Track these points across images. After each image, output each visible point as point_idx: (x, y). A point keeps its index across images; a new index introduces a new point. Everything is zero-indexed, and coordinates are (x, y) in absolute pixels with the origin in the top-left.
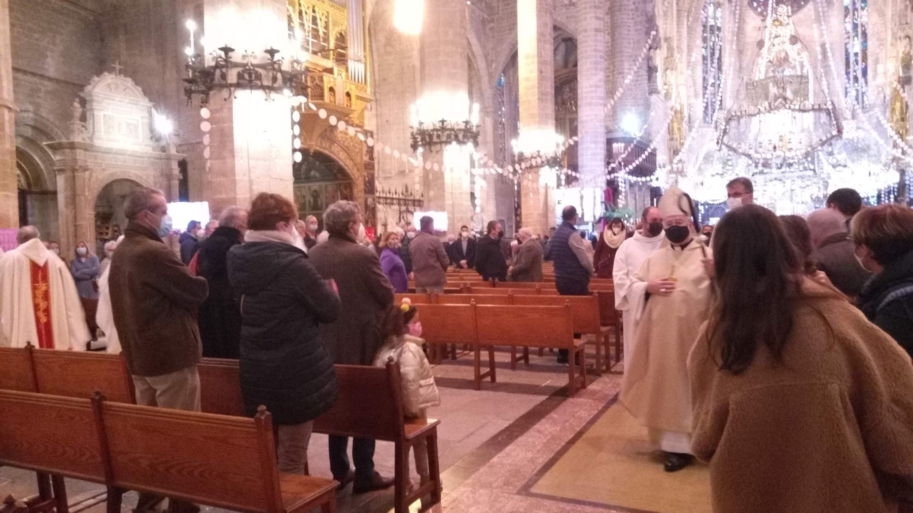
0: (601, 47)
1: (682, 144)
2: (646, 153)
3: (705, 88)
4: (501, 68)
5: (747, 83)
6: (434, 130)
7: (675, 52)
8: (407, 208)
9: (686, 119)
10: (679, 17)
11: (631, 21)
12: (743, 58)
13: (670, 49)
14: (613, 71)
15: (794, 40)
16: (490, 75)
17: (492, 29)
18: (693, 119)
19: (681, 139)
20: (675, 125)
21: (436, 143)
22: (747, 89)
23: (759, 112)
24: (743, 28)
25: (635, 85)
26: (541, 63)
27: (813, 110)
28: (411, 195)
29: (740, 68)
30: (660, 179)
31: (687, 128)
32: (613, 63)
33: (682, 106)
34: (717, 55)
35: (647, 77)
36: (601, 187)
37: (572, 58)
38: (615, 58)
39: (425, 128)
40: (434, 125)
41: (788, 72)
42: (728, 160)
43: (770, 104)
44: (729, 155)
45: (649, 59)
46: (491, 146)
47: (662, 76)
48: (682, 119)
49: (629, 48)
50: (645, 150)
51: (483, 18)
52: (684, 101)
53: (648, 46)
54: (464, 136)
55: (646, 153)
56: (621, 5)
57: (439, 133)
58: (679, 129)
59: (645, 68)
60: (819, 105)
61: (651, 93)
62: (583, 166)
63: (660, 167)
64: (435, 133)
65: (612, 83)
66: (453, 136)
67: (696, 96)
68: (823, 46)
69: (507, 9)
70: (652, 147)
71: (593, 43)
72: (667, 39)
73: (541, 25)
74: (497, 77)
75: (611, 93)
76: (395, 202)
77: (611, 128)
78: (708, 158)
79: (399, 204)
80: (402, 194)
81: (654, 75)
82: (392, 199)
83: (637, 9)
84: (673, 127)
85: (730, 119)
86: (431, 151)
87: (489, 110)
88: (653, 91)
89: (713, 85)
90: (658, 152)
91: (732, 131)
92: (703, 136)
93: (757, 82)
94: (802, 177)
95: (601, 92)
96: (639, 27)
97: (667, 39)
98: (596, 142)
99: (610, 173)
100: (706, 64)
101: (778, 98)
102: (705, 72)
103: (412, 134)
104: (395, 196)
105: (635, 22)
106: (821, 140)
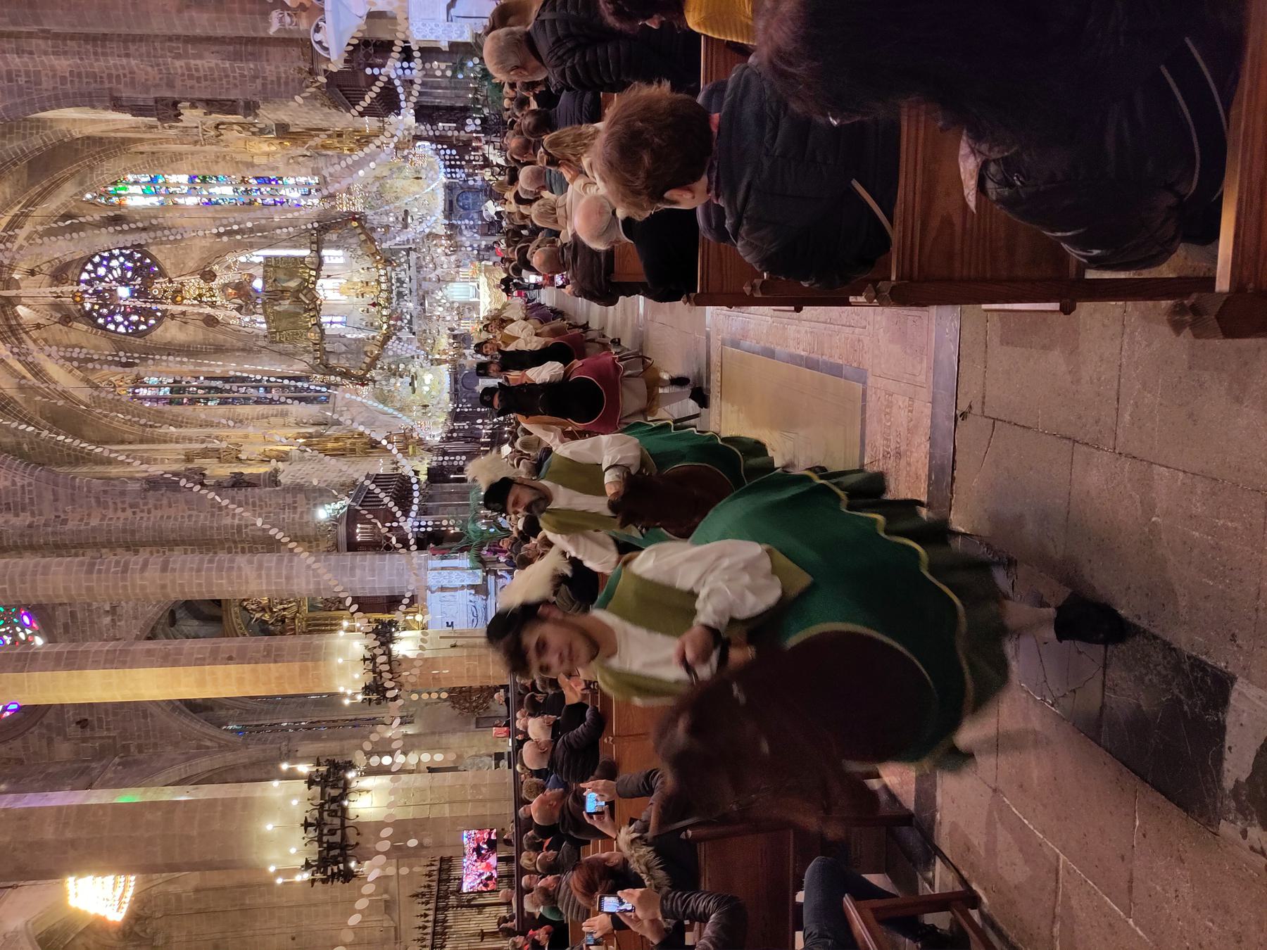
0: (193, 559)
1: (361, 434)
2: (372, 487)
3: (271, 401)
4: (213, 731)
5: (272, 342)
6: (320, 841)
7: (210, 446)
8: (453, 893)
9: (321, 429)
10: (152, 441)
11: (152, 515)
12: (228, 345)
13: (205, 454)
14: (235, 542)
15: (208, 276)
16: (224, 747)
17: (140, 749)
18: (321, 420)
19: (353, 437)
20: (330, 445)
21: (344, 836)
22: (281, 342)
23: (319, 325)
24: (180, 345)
25: (260, 506)
26: (215, 658)
27: (318, 251)
28: (429, 886)
29: (243, 350)
30: (417, 467)
31: (335, 427)
32: (221, 542)
33: (300, 436)
34: (219, 384)
35: (249, 489)
36: (426, 559)
37: (206, 610)
38: (213, 540)
39: (316, 857)
40: (312, 840)
41: (258, 284)
42: (390, 369)
43: (306, 311)
44: (382, 368)
45: (219, 486)
46: (347, 744)
47: (250, 465)
48: (321, 435)
49: (198, 516)
50: (370, 492)
51: (119, 765)
52: (292, 432)
53: (198, 487)
54: (334, 787)
55: (372, 487)
56: (124, 531)
57: (325, 831)
58: (337, 440)
59: (232, 492)
60: (313, 243)
61: (276, 483)
62: (392, 589)
63: (397, 469)
64: (325, 839)
65: (255, 543)
66: (334, 806)
67: (284, 414)
68: (219, 235)
69: (108, 723)
70: (362, 479)
71: (186, 575)
72: (189, 459)
73: (150, 660)
74: (228, 736)
75: (272, 545)
76: (441, 917)
77: (330, 543)
78: (384, 399)
79: (446, 908)
80: (427, 903)
81: (247, 478)
82: (435, 921)
83: (131, 506)
84: (334, 450)
85: (326, 366)
86: (357, 844)
87: (284, 749)
88: (273, 479)
89: (268, 390)
90: (373, 472)
91: (342, 363)
92: (349, 404)
93: (269, 328)
94: (419, 268)
95: (270, 560)
96: (165, 502)
97: (189, 459)
98: (353, 568)
99: (406, 545)
100: (234, 399)
101: (298, 298)
102: (246, 400)
103: (324, 881)
104: (431, 918)
105: (156, 509)
106: (365, 241)
